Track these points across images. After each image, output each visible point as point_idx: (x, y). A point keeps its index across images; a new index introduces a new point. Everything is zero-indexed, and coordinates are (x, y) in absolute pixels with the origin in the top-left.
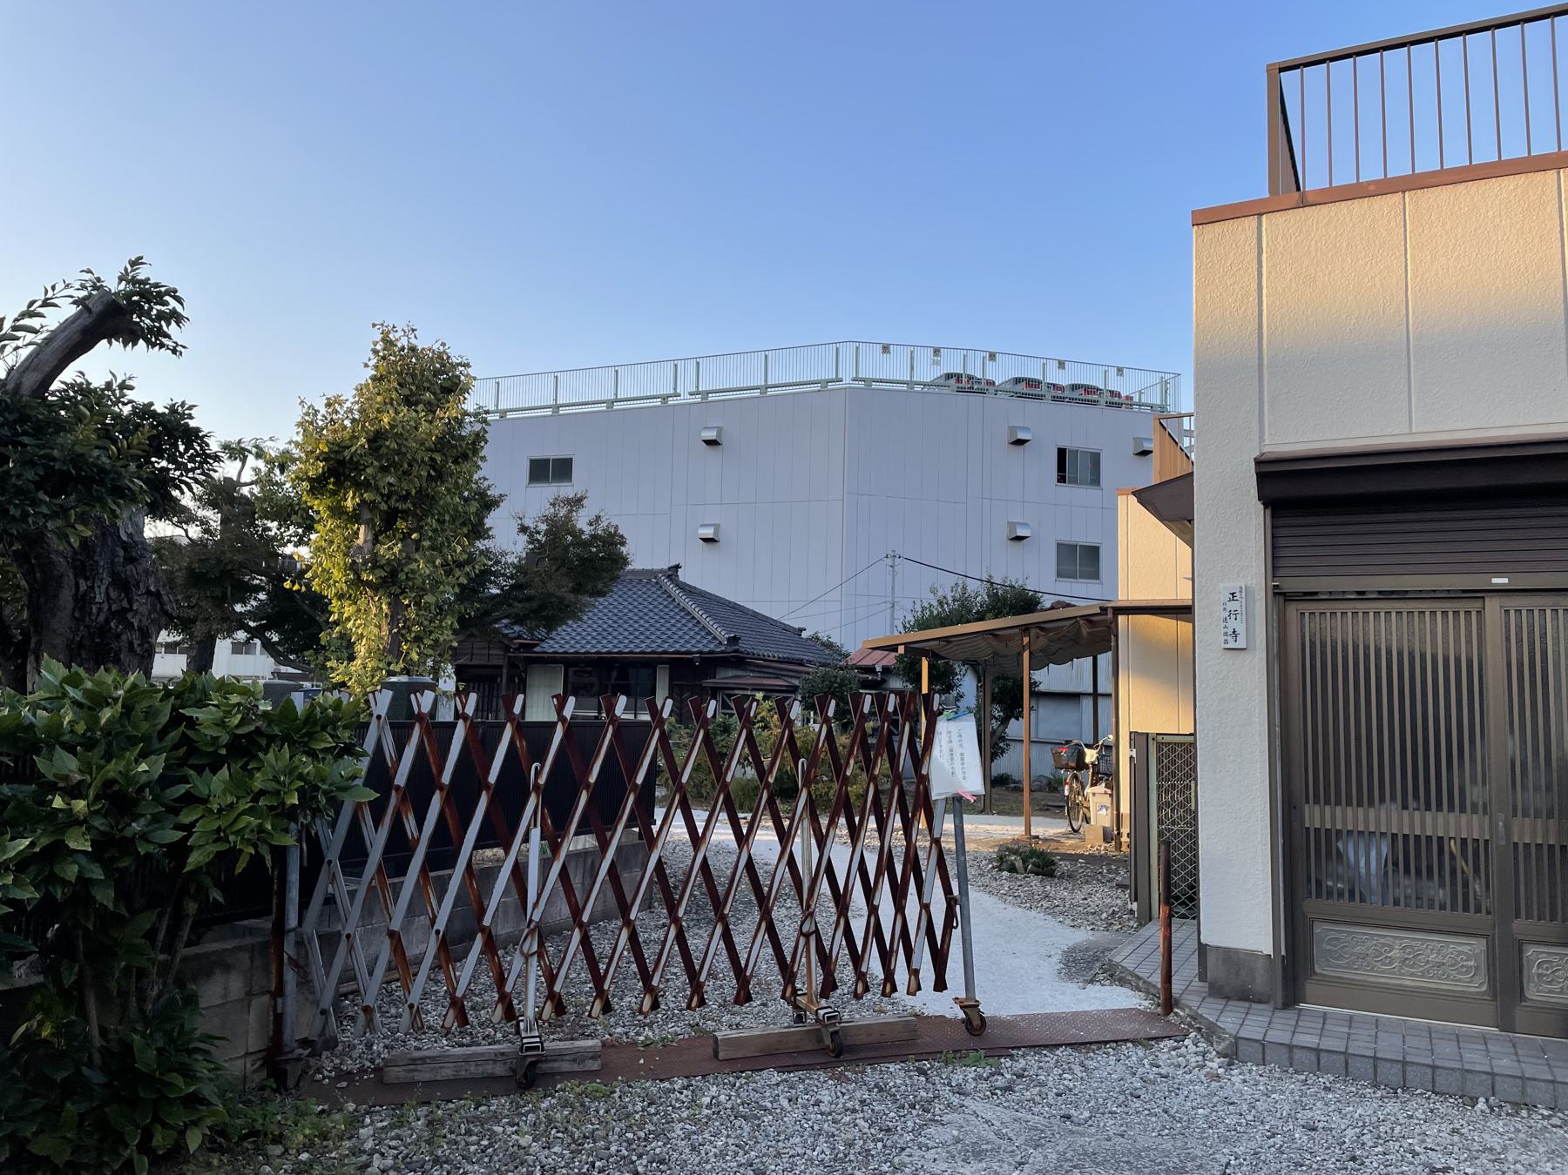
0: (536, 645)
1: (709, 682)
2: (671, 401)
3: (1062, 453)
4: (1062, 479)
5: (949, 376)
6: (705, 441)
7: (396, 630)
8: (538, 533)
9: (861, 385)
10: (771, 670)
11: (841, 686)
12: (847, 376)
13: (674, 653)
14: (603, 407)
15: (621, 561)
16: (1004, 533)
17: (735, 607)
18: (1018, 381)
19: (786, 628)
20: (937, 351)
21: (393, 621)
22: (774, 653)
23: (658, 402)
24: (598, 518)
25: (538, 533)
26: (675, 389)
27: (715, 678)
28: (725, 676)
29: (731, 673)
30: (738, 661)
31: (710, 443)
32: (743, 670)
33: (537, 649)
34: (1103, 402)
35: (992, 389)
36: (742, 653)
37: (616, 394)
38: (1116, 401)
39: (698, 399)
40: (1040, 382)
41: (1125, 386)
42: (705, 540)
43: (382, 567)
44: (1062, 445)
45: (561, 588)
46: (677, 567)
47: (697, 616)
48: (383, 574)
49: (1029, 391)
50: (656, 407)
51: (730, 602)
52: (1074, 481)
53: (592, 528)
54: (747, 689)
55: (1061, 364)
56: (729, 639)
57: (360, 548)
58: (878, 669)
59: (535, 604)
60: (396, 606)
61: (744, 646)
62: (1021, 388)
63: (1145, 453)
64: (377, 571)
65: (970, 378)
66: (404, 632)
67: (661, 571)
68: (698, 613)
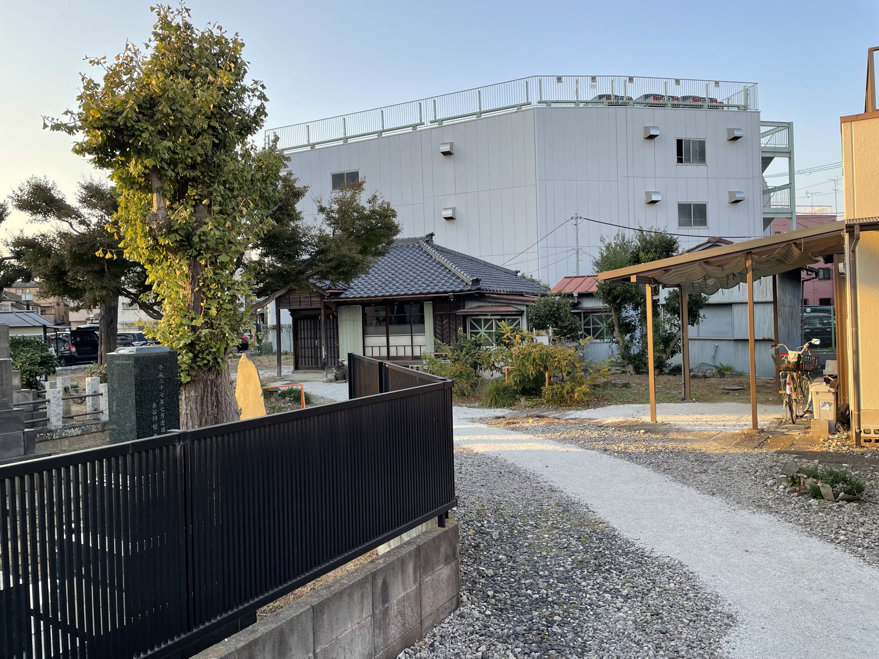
0: (342, 293)
1: (461, 312)
2: (419, 128)
3: (679, 142)
4: (680, 160)
5: (601, 97)
6: (442, 153)
7: (197, 289)
8: (332, 211)
9: (544, 105)
10: (503, 301)
11: (558, 309)
12: (534, 100)
13: (435, 293)
14: (375, 136)
15: (393, 229)
16: (643, 199)
17: (471, 260)
18: (647, 96)
19: (507, 272)
20: (594, 79)
21: (194, 281)
22: (502, 288)
23: (410, 130)
24: (375, 197)
25: (332, 211)
26: (421, 120)
27: (464, 308)
28: (471, 307)
29: (475, 304)
30: (480, 296)
31: (446, 154)
32: (483, 301)
33: (342, 296)
34: (706, 105)
35: (631, 102)
36: (483, 290)
37: (383, 127)
38: (714, 105)
39: (436, 125)
40: (663, 96)
41: (720, 95)
42: (447, 219)
43: (176, 231)
44: (680, 137)
45: (352, 251)
46: (432, 235)
47: (448, 266)
48: (178, 238)
49: (656, 102)
50: (410, 133)
51: (468, 256)
52: (688, 160)
53: (371, 205)
54: (488, 315)
55: (677, 82)
56: (473, 281)
57: (155, 215)
58: (575, 295)
59: (333, 264)
60: (194, 266)
61: (483, 285)
62: (651, 100)
63: (736, 138)
64: (172, 236)
65: (616, 96)
66: (204, 290)
67: (421, 238)
68: (449, 265)
